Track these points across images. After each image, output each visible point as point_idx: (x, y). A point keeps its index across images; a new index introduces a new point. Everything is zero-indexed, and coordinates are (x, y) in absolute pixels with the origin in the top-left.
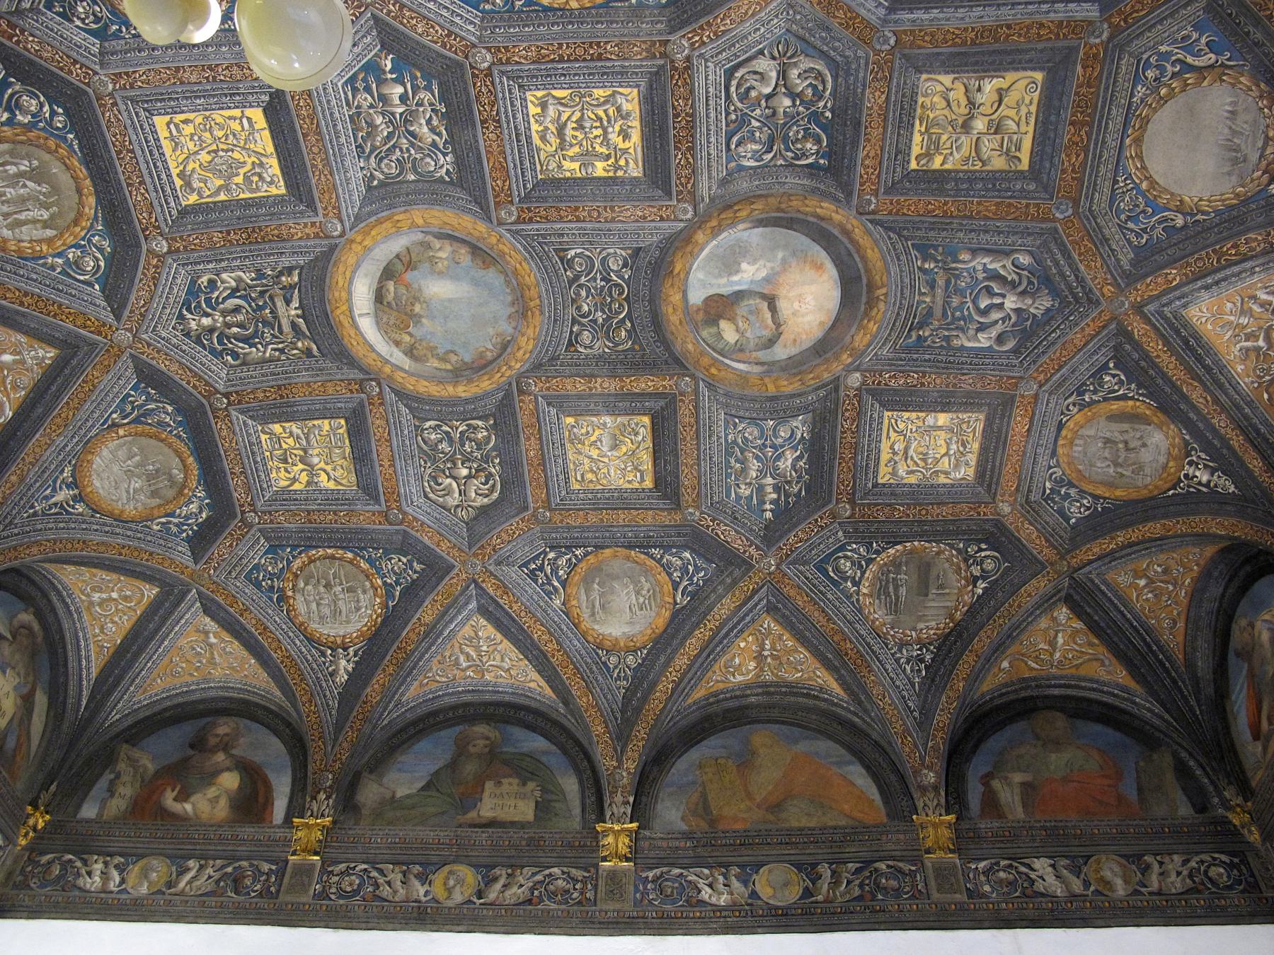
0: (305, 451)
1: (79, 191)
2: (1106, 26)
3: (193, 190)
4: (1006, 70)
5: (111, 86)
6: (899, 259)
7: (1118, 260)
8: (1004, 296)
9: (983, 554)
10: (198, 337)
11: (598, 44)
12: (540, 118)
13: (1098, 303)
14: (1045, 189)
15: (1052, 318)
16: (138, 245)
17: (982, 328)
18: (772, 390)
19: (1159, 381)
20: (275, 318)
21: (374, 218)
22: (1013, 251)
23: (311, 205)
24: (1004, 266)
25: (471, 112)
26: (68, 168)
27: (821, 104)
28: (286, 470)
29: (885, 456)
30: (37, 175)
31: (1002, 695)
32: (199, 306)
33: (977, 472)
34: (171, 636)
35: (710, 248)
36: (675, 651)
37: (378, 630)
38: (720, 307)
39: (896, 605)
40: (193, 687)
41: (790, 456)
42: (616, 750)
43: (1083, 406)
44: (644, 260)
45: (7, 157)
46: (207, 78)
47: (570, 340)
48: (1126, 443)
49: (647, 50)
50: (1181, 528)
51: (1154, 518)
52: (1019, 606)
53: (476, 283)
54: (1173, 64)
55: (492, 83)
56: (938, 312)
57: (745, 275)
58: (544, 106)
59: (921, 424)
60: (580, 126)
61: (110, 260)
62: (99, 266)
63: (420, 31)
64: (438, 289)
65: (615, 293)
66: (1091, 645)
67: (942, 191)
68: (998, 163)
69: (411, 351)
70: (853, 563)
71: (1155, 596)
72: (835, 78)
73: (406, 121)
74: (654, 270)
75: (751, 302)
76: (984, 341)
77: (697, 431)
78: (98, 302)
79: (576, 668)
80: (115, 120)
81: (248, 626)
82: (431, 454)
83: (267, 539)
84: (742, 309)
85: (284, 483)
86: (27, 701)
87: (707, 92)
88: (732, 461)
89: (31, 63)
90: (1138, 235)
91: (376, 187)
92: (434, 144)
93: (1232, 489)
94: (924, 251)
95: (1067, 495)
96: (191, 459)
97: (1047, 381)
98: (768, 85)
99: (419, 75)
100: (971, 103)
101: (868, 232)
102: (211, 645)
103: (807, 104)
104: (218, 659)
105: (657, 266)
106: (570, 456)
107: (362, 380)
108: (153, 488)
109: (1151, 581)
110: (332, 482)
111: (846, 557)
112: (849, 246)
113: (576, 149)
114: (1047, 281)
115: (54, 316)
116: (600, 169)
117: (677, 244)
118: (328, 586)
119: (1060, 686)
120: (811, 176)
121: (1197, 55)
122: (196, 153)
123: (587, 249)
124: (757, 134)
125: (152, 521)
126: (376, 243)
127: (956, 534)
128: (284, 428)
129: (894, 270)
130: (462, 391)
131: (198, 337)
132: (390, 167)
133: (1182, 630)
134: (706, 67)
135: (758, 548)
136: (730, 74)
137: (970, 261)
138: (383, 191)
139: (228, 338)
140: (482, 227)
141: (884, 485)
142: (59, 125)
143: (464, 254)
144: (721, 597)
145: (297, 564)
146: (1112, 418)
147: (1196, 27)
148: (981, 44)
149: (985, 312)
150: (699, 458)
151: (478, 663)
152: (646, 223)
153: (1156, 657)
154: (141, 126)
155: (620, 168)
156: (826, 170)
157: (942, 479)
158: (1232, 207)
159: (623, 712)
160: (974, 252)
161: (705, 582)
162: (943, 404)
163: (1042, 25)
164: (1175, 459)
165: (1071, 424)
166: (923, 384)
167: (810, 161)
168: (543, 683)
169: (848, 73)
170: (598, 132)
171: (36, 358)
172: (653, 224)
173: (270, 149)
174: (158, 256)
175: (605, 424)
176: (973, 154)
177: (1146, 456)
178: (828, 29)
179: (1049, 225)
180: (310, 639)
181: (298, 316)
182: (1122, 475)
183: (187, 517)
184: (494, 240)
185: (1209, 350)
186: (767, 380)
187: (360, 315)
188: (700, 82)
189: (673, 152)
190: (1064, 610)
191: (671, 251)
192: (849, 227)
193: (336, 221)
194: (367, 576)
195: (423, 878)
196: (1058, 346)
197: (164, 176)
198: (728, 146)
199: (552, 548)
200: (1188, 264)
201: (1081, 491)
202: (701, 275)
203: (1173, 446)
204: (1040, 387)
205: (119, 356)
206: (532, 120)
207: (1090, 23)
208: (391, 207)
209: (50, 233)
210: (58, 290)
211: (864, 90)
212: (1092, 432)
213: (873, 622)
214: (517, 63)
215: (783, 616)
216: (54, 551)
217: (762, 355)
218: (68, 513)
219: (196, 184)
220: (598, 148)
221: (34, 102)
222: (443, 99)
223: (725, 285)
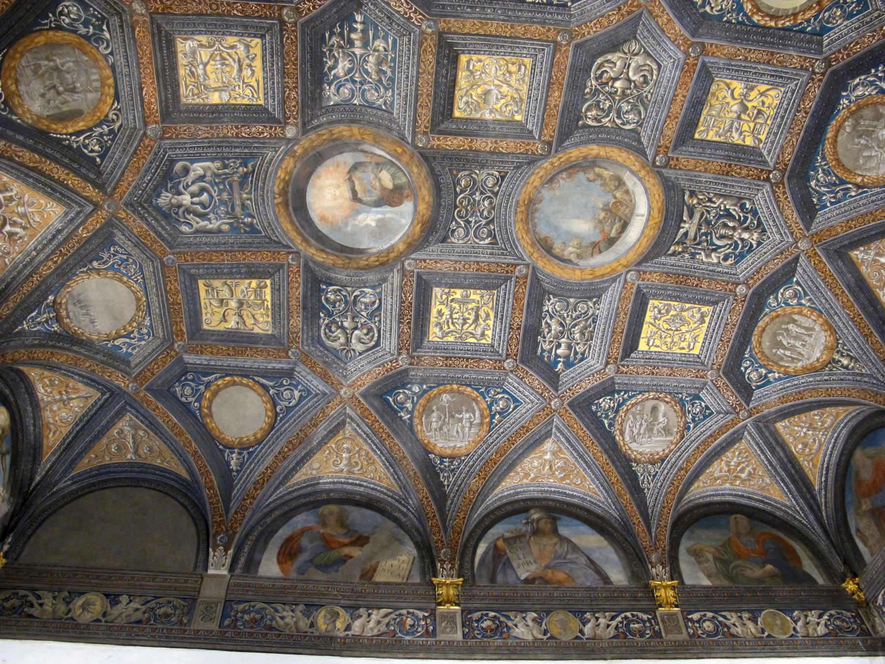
0: (739, 117)
1: (764, 330)
6: (269, 223)
7: (123, 235)
8: (192, 203)
11: (446, 366)
13: (126, 204)
14: (184, 271)
15: (155, 190)
16: (753, 294)
17: (202, 178)
18: (355, 129)
19: (58, 156)
22: (194, 233)
23: (639, 290)
24: (197, 223)
25: (524, 335)
26: (760, 343)
27: (326, 321)
28: (763, 103)
29: (258, 64)
30: (780, 345)
32: (743, 247)
33: (174, 46)
35: (395, 240)
38: (391, 197)
43: (106, 121)
44: (440, 234)
45: (785, 358)
47: (502, 180)
48: (59, 93)
49: (421, 361)
53: (556, 228)
56: (236, 186)
57: (373, 217)
58: (483, 335)
60: (465, 320)
61: (776, 291)
65: (463, 213)
67: (248, 266)
68: (217, 283)
72: (319, 336)
73: (562, 333)
74: (436, 226)
75: (369, 199)
76: (198, 168)
77: (416, 101)
80: (721, 356)
83: (820, 43)
84: (376, 194)
85: (773, 93)
88: (389, 73)
89: (739, 392)
90: (117, 252)
91: (595, 297)
92: (551, 317)
94: (253, 229)
95: (86, 24)
96: (829, 136)
97: (141, 140)
98: (356, 335)
100: (241, 316)
101: (292, 241)
103: (334, 322)
105: (433, 230)
106: (525, 88)
107: (665, 167)
108: (875, 123)
110: (732, 87)
112: (302, 231)
113: (470, 306)
114: (166, 216)
116: (458, 294)
117: (417, 243)
120: (330, 278)
121: (124, 343)
122: (687, 332)
124: (363, 307)
126: (611, 262)
128: (744, 140)
129: (271, 216)
130: (594, 150)
131: (758, 226)
132: (582, 308)
136: (378, 344)
137: (221, 225)
138: (592, 294)
139: (739, 220)
140: (540, 264)
141: (255, 36)
143: (557, 249)
146: (76, 114)
147: (131, 354)
149: (203, 190)
150: (418, 78)
152: (435, 259)
155: (446, 294)
156: (321, 282)
157: (204, 39)
158: (69, 280)
160: (219, 231)
162: (217, 113)
163: (212, 353)
164: (13, 93)
165: (110, 101)
166: (237, 128)
167: (331, 288)
169: (313, 339)
170: (455, 316)
171: (867, 254)
173: (645, 326)
174: (746, 284)
175: (491, 112)
184: (536, 255)
185: (34, 187)
186: (359, 137)
187: (643, 215)
188: (394, 341)
189: (413, 301)
192: (304, 245)
193: (629, 280)
196: (143, 170)
197: (713, 324)
200: (78, 242)
201: (75, 32)
202: (403, 221)
203: (21, 105)
204: (145, 134)
205: (817, 234)
206: (491, 327)
207: (186, 352)
208: (591, 284)
210: (817, 287)
212: (90, 96)
217: (362, 158)
219: (698, 316)
223: (387, 212)
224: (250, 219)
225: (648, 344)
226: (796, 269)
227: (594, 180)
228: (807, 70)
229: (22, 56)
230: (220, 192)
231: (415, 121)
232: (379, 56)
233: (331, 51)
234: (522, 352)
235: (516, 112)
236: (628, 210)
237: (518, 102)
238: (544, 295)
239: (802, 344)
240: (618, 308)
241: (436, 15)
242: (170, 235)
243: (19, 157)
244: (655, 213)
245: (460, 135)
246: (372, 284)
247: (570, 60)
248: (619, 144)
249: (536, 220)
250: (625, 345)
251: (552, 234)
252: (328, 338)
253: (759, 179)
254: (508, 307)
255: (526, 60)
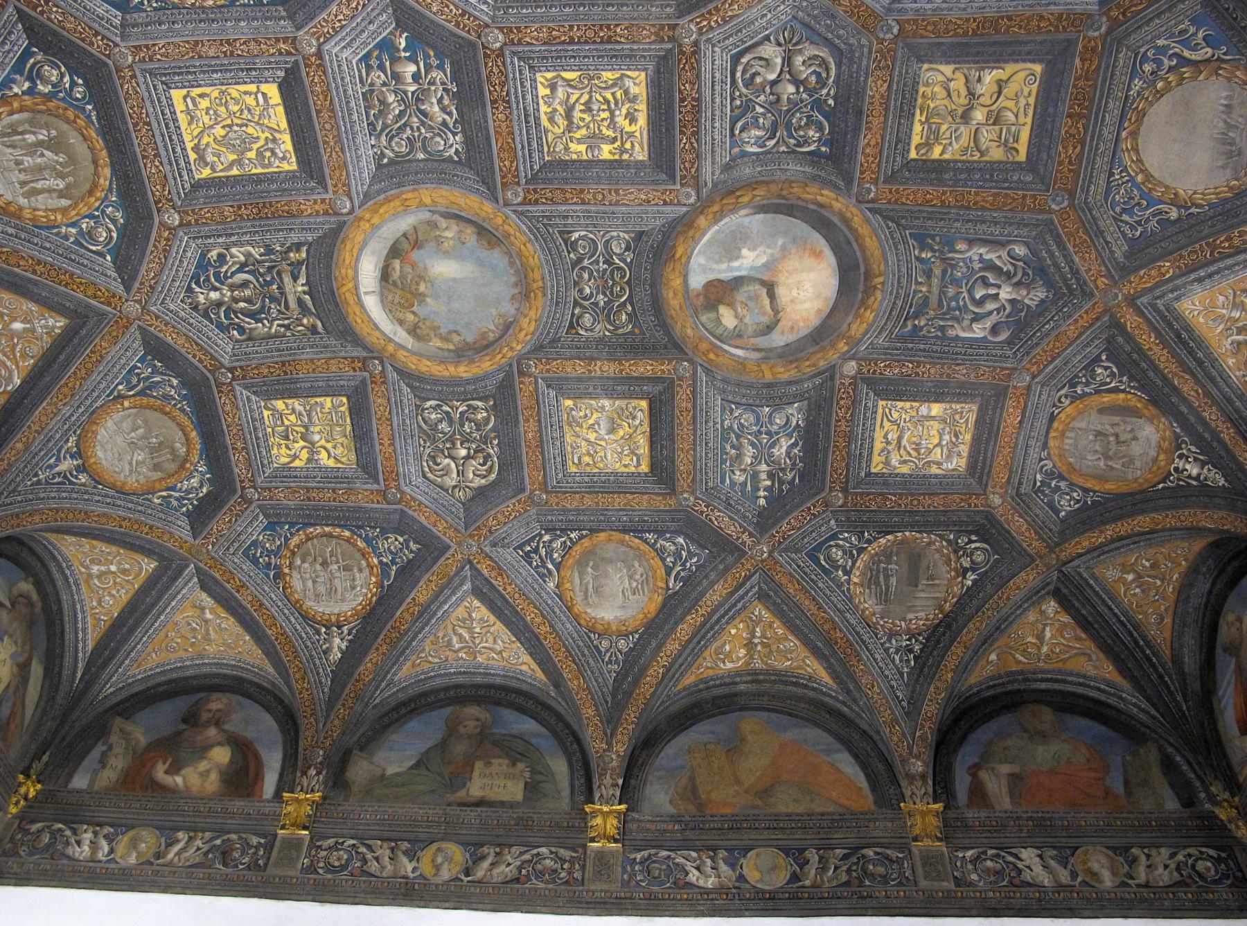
0: (307, 428)
2: (1104, 19)
3: (207, 164)
4: (1006, 61)
5: (130, 59)
6: (896, 248)
7: (1112, 252)
8: (999, 287)
9: (973, 546)
10: (206, 311)
12: (549, 100)
13: (1092, 295)
14: (1042, 181)
15: (1046, 309)
17: (977, 318)
19: (1151, 374)
20: (282, 294)
21: (383, 196)
23: (322, 182)
24: (1000, 257)
27: (824, 92)
29: (878, 445)
30: (55, 145)
31: (988, 688)
32: (207, 279)
34: (168, 610)
36: (667, 636)
37: (373, 609)
38: (720, 292)
39: (886, 595)
40: (188, 663)
41: (784, 444)
42: (606, 734)
43: (1074, 398)
45: (27, 126)
46: (225, 53)
47: (571, 322)
48: (1117, 435)
49: (656, 34)
50: (1171, 522)
51: (1143, 512)
52: (1008, 599)
53: (480, 263)
54: (1170, 58)
55: (504, 63)
57: (745, 262)
58: (553, 87)
59: (914, 414)
60: (588, 109)
61: (123, 231)
62: (111, 237)
63: (435, 9)
64: (444, 269)
65: (617, 277)
66: (1078, 639)
67: (941, 182)
68: (996, 154)
69: (414, 330)
70: (845, 553)
71: (1143, 591)
72: (839, 65)
73: (418, 99)
75: (751, 288)
76: (979, 331)
78: (109, 273)
79: (568, 650)
80: (133, 91)
81: (244, 603)
82: (431, 434)
84: (741, 295)
85: (284, 460)
86: (23, 669)
87: (713, 77)
89: (54, 34)
90: (1132, 228)
92: (444, 124)
93: (1222, 482)
95: (1058, 488)
96: (194, 434)
97: (1040, 372)
98: (773, 71)
99: (432, 53)
100: (971, 94)
101: (867, 220)
102: (206, 621)
103: (811, 91)
104: (213, 635)
105: (659, 250)
106: (569, 438)
107: (365, 359)
108: (155, 461)
109: (1139, 576)
111: (837, 546)
112: (848, 233)
114: (1042, 272)
115: (66, 286)
116: (606, 152)
117: (679, 228)
118: (325, 564)
119: (1047, 680)
120: (813, 164)
122: (211, 127)
123: (591, 232)
124: (761, 120)
125: (153, 494)
127: (946, 525)
128: (286, 405)
129: (892, 259)
130: (463, 371)
133: (1170, 625)
134: (713, 52)
135: (751, 535)
136: (736, 59)
137: (967, 251)
139: (235, 313)
140: (488, 207)
142: (79, 96)
143: (470, 233)
144: (712, 584)
145: (294, 541)
148: (982, 34)
149: (980, 303)
151: (471, 644)
152: (649, 207)
153: (1143, 652)
154: (159, 99)
155: (626, 151)
156: (828, 157)
157: (934, 470)
159: (614, 695)
160: (971, 242)
161: (698, 568)
162: (938, 394)
163: (1042, 18)
164: (1165, 453)
165: (1062, 416)
167: (812, 148)
168: (534, 666)
169: (851, 60)
170: (606, 115)
171: (46, 327)
172: (655, 208)
174: (170, 229)
175: (603, 408)
176: (972, 144)
177: (1136, 449)
178: (833, 17)
179: (1045, 216)
180: (306, 617)
181: (305, 293)
182: (1112, 468)
183: (188, 492)
185: (1200, 343)
186: (764, 367)
187: (366, 293)
188: (706, 67)
189: (678, 136)
190: (1052, 603)
191: (673, 236)
192: (849, 215)
193: (345, 199)
194: (363, 555)
195: (411, 855)
196: (1051, 338)
197: (178, 149)
198: (732, 130)
199: (547, 531)
200: (1181, 257)
201: (1072, 484)
202: (702, 260)
203: (1164, 439)
204: (1033, 377)
206: (541, 102)
207: (1090, 16)
208: (400, 185)
209: (65, 202)
211: (866, 79)
212: (1083, 425)
213: (863, 611)
214: (528, 44)
215: (775, 603)
216: (56, 520)
217: (761, 342)
218: (71, 483)
219: (210, 158)
220: (604, 131)
221: (55, 72)
222: (455, 78)
223: (724, 271)
224: (924, 256)
225: (264, 95)
226: (118, 270)
227: (450, 332)
228: (264, 489)
229: (1136, 480)
230: (956, 297)
231: (694, 392)
232: (740, 464)
233: (794, 464)
234: (477, 63)
235: (572, 409)
236: (390, 298)
237: (573, 422)
238: (469, 159)
239: (21, 163)
240: (343, 150)
241: (680, 511)
242: (1045, 242)
243: (1197, 391)
244: (351, 299)
245: (637, 378)
246: (746, 159)
247: (526, 475)
248: (436, 381)
249: (512, 272)
250: (304, 89)
251: (483, 254)
252: (824, 63)
253: (241, 367)
254: (520, 138)
255: (574, 469)
